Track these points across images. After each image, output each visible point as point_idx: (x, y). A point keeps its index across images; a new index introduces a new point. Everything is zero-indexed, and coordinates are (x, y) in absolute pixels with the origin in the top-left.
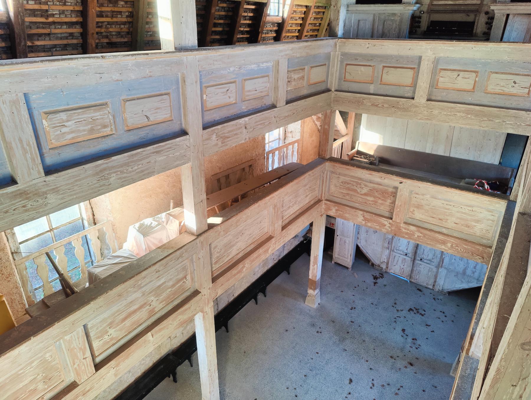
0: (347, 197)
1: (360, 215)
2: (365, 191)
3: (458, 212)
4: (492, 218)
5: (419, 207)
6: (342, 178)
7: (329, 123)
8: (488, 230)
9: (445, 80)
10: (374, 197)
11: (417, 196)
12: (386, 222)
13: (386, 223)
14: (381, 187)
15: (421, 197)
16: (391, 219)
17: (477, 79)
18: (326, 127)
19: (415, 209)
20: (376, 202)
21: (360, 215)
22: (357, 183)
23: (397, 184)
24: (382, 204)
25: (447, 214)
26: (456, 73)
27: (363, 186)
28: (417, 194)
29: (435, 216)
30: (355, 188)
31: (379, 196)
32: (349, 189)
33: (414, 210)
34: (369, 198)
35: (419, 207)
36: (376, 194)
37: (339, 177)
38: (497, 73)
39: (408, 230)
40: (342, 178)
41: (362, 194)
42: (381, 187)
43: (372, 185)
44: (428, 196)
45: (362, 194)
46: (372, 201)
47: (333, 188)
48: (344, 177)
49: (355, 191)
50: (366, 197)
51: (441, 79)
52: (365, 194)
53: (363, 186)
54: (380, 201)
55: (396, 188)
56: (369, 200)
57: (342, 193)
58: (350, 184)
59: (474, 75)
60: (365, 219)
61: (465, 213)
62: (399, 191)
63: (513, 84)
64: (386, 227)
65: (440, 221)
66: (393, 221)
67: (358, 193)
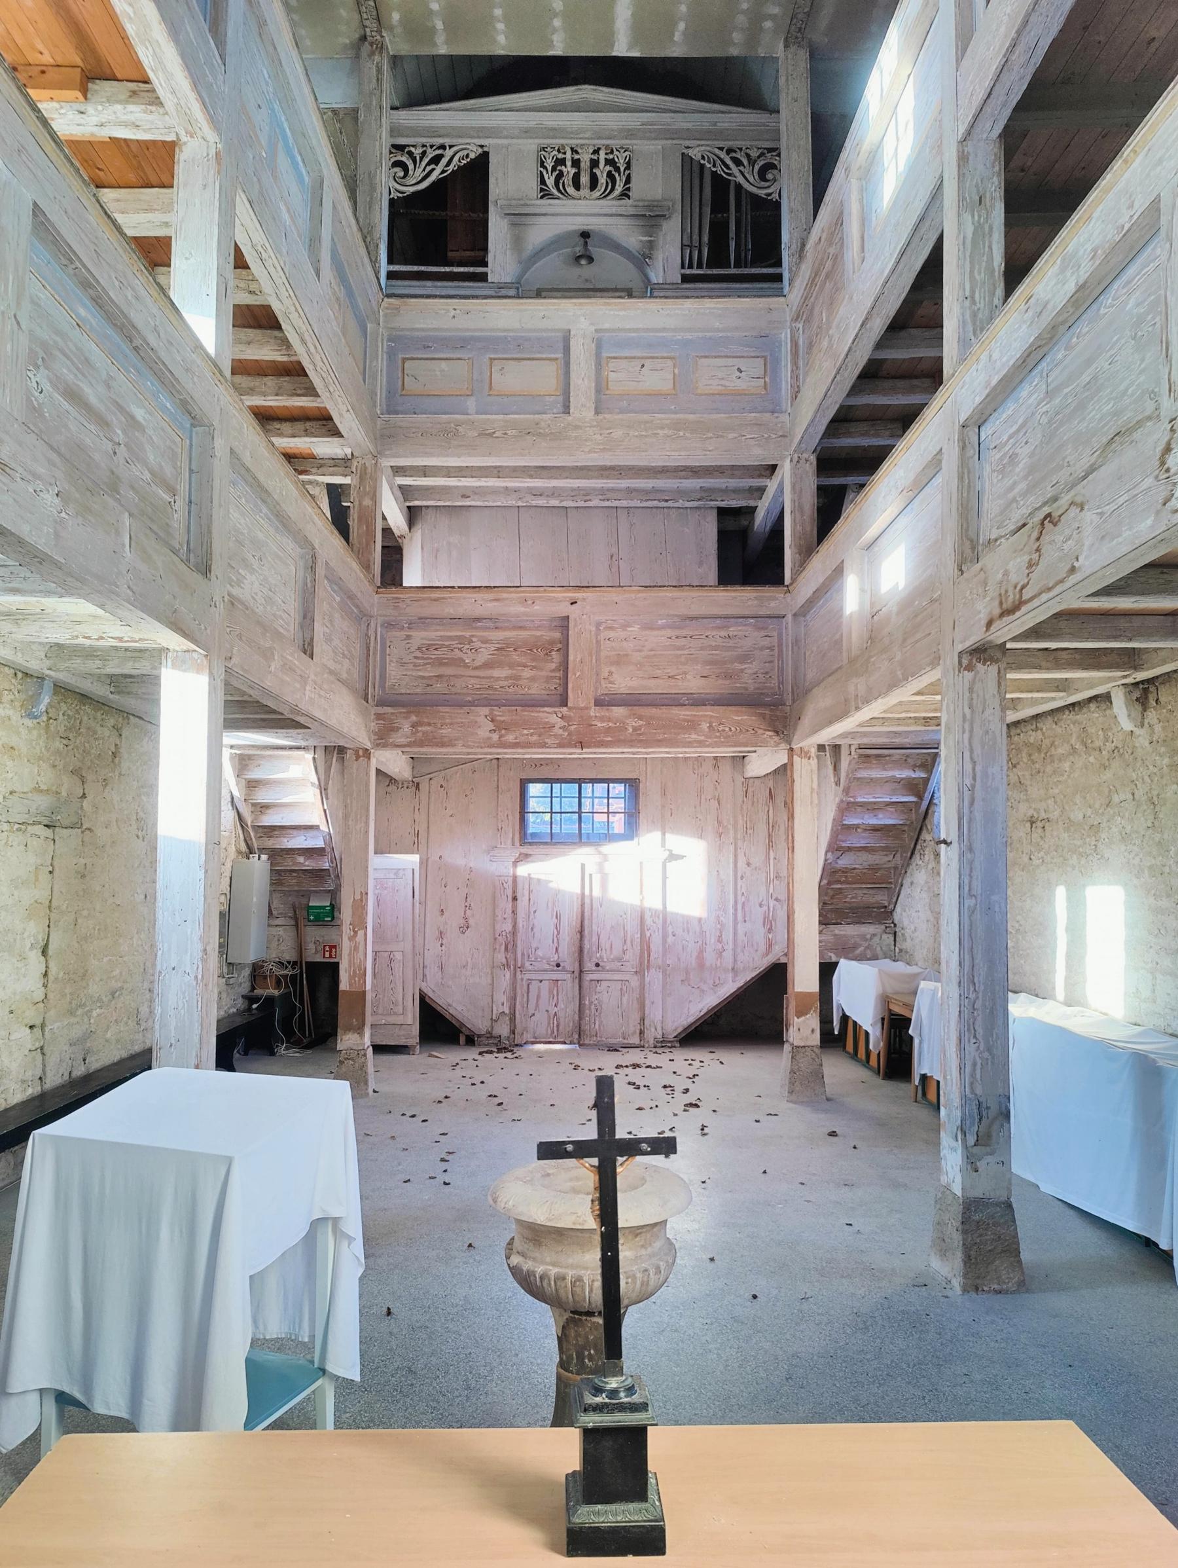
0: (439, 687)
1: (481, 719)
2: (484, 655)
3: (702, 649)
4: (766, 642)
5: (620, 660)
6: (420, 636)
7: (375, 492)
8: (767, 673)
9: (620, 378)
10: (511, 666)
11: (612, 634)
12: (551, 716)
13: (554, 719)
14: (524, 634)
15: (622, 634)
16: (564, 703)
17: (676, 371)
18: (367, 502)
19: (613, 669)
20: (517, 678)
21: (481, 719)
22: (461, 640)
23: (564, 609)
24: (533, 679)
25: (683, 660)
26: (638, 363)
27: (478, 644)
28: (611, 628)
29: (658, 673)
30: (460, 654)
31: (523, 660)
32: (440, 662)
33: (611, 673)
34: (496, 673)
35: (620, 660)
36: (515, 657)
37: (408, 637)
38: (706, 357)
39: (609, 720)
40: (420, 636)
41: (476, 668)
42: (524, 634)
43: (501, 635)
44: (636, 628)
45: (476, 668)
46: (506, 678)
47: (393, 671)
48: (423, 634)
49: (459, 663)
50: (488, 673)
51: (612, 376)
52: (487, 665)
53: (478, 644)
54: (527, 673)
55: (564, 623)
56: (498, 679)
57: (423, 677)
58: (442, 646)
59: (670, 363)
60: (499, 727)
61: (716, 648)
62: (571, 625)
63: (738, 374)
64: (557, 730)
65: (672, 682)
66: (570, 709)
67: (466, 666)
